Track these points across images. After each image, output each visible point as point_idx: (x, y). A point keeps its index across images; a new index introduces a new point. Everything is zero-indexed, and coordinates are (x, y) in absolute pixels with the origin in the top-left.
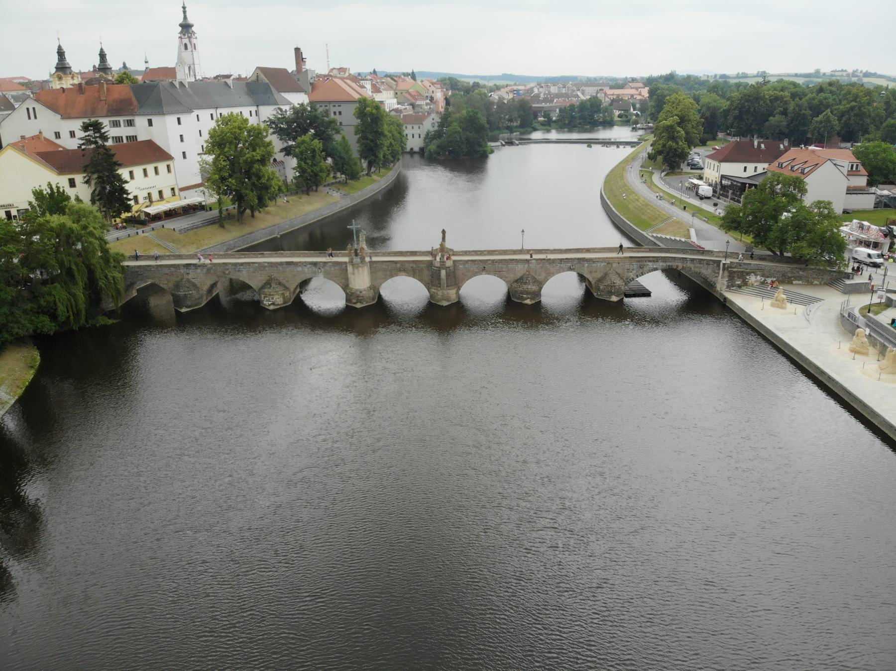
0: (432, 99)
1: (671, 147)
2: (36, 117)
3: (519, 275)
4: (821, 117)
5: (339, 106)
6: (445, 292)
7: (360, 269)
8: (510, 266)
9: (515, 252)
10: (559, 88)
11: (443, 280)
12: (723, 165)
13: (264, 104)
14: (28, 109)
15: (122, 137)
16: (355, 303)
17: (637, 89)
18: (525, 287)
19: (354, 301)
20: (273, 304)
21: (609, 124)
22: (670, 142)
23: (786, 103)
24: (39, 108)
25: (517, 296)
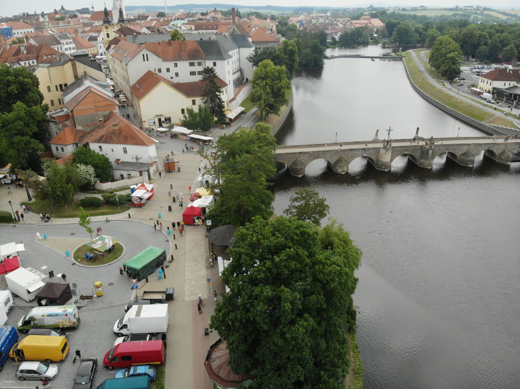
0: (272, 30)
1: (454, 69)
2: (148, 60)
3: (464, 152)
4: (508, 48)
5: (267, 44)
6: (430, 161)
7: (389, 151)
8: (461, 147)
9: (454, 139)
10: (325, 19)
12: (495, 82)
14: (143, 55)
15: (195, 72)
17: (368, 19)
18: (469, 158)
19: (383, 168)
21: (365, 44)
22: (453, 66)
23: (486, 38)
24: (150, 55)
25: (464, 163)
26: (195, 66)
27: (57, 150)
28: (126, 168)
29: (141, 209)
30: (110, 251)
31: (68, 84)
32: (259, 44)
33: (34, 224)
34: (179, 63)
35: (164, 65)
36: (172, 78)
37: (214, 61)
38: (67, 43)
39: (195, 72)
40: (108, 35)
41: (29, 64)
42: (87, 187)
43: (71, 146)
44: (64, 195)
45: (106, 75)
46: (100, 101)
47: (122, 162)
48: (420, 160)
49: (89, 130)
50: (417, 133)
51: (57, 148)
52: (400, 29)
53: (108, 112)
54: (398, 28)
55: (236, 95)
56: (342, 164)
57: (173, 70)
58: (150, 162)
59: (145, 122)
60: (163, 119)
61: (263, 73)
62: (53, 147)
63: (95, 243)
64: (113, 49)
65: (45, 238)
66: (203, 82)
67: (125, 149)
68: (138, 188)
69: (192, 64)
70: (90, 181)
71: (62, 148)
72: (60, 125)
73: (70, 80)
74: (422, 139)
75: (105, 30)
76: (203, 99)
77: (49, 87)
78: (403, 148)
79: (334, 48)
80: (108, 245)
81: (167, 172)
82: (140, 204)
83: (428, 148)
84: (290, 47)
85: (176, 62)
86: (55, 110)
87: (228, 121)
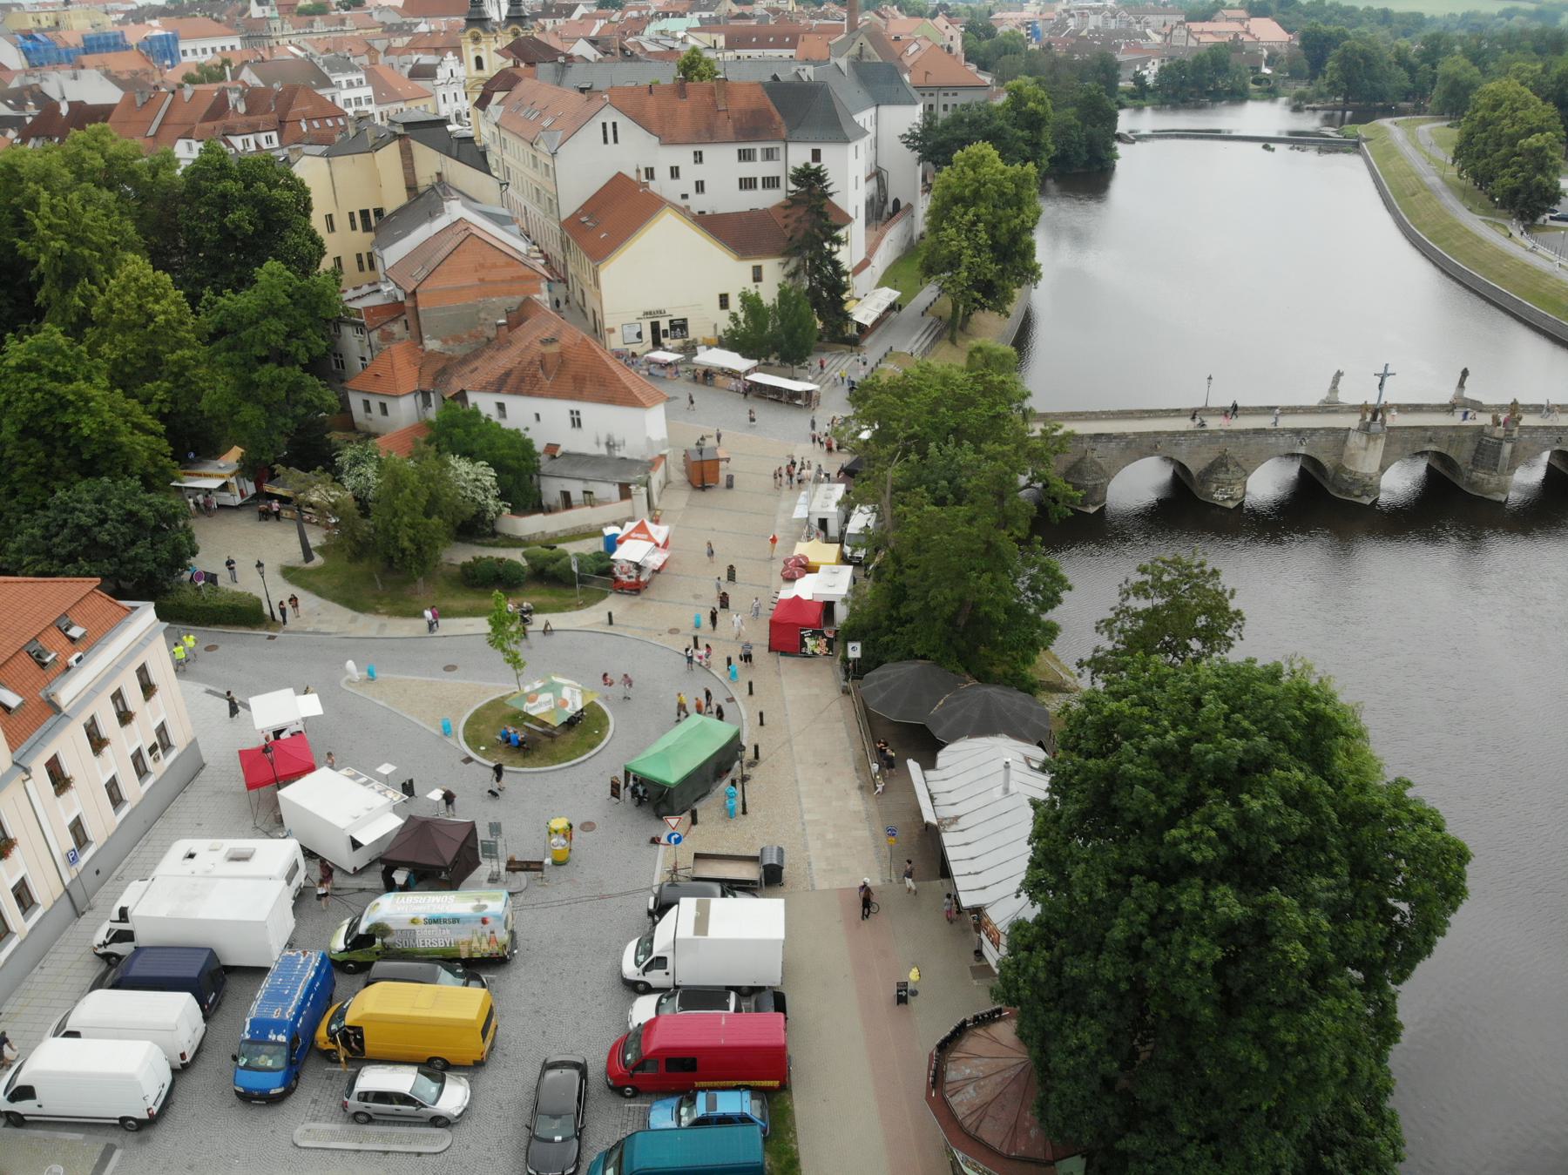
0: (950, 49)
2: (616, 141)
5: (955, 94)
7: (1379, 441)
10: (1105, 18)
11: (1504, 459)
13: (890, 102)
14: (604, 125)
15: (755, 179)
16: (1358, 496)
17: (1241, 21)
19: (1357, 492)
20: (1231, 499)
21: (1238, 96)
24: (624, 123)
26: (754, 160)
27: (368, 409)
28: (579, 473)
29: (638, 598)
30: (571, 723)
31: (388, 211)
32: (931, 95)
33: (329, 634)
34: (708, 151)
35: (664, 158)
36: (685, 196)
37: (816, 147)
38: (350, 84)
39: (755, 179)
40: (479, 63)
41: (257, 145)
42: (474, 527)
43: (410, 398)
44: (419, 549)
45: (501, 185)
46: (494, 266)
47: (565, 454)
48: (1472, 471)
49: (459, 351)
50: (1461, 385)
51: (367, 403)
52: (1349, 55)
53: (519, 299)
54: (1345, 51)
55: (871, 251)
56: (1229, 476)
57: (690, 173)
58: (650, 458)
59: (612, 331)
60: (664, 325)
61: (966, 186)
62: (356, 402)
63: (532, 700)
64: (498, 104)
65: (371, 678)
66: (788, 212)
67: (575, 416)
68: (628, 536)
69: (745, 156)
70: (483, 510)
71: (383, 407)
72: (375, 335)
73: (394, 197)
74: (1478, 407)
75: (471, 47)
76: (785, 265)
77: (330, 216)
78: (1422, 433)
79: (1139, 108)
80: (570, 706)
81: (695, 488)
82: (636, 586)
83: (1502, 435)
84: (1031, 105)
85: (698, 148)
86: (355, 289)
87: (852, 331)
